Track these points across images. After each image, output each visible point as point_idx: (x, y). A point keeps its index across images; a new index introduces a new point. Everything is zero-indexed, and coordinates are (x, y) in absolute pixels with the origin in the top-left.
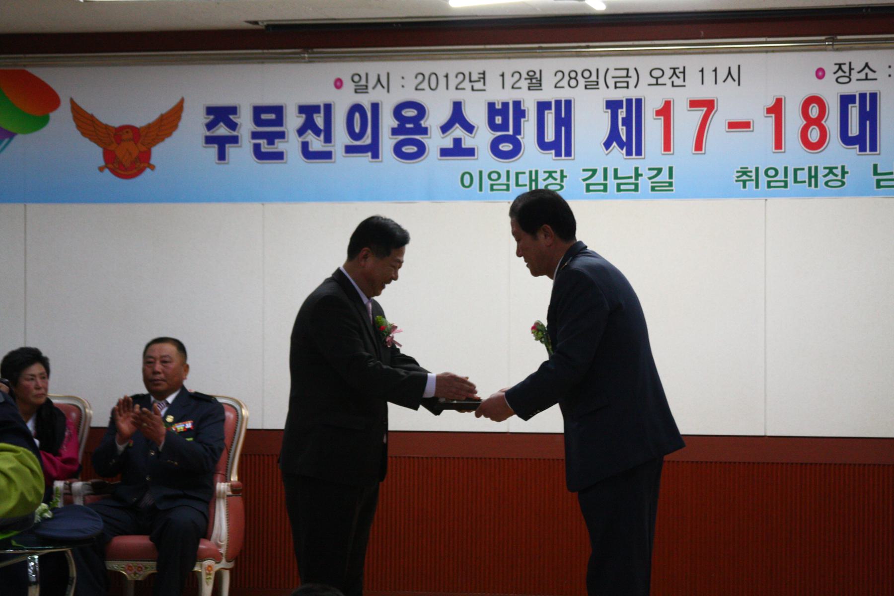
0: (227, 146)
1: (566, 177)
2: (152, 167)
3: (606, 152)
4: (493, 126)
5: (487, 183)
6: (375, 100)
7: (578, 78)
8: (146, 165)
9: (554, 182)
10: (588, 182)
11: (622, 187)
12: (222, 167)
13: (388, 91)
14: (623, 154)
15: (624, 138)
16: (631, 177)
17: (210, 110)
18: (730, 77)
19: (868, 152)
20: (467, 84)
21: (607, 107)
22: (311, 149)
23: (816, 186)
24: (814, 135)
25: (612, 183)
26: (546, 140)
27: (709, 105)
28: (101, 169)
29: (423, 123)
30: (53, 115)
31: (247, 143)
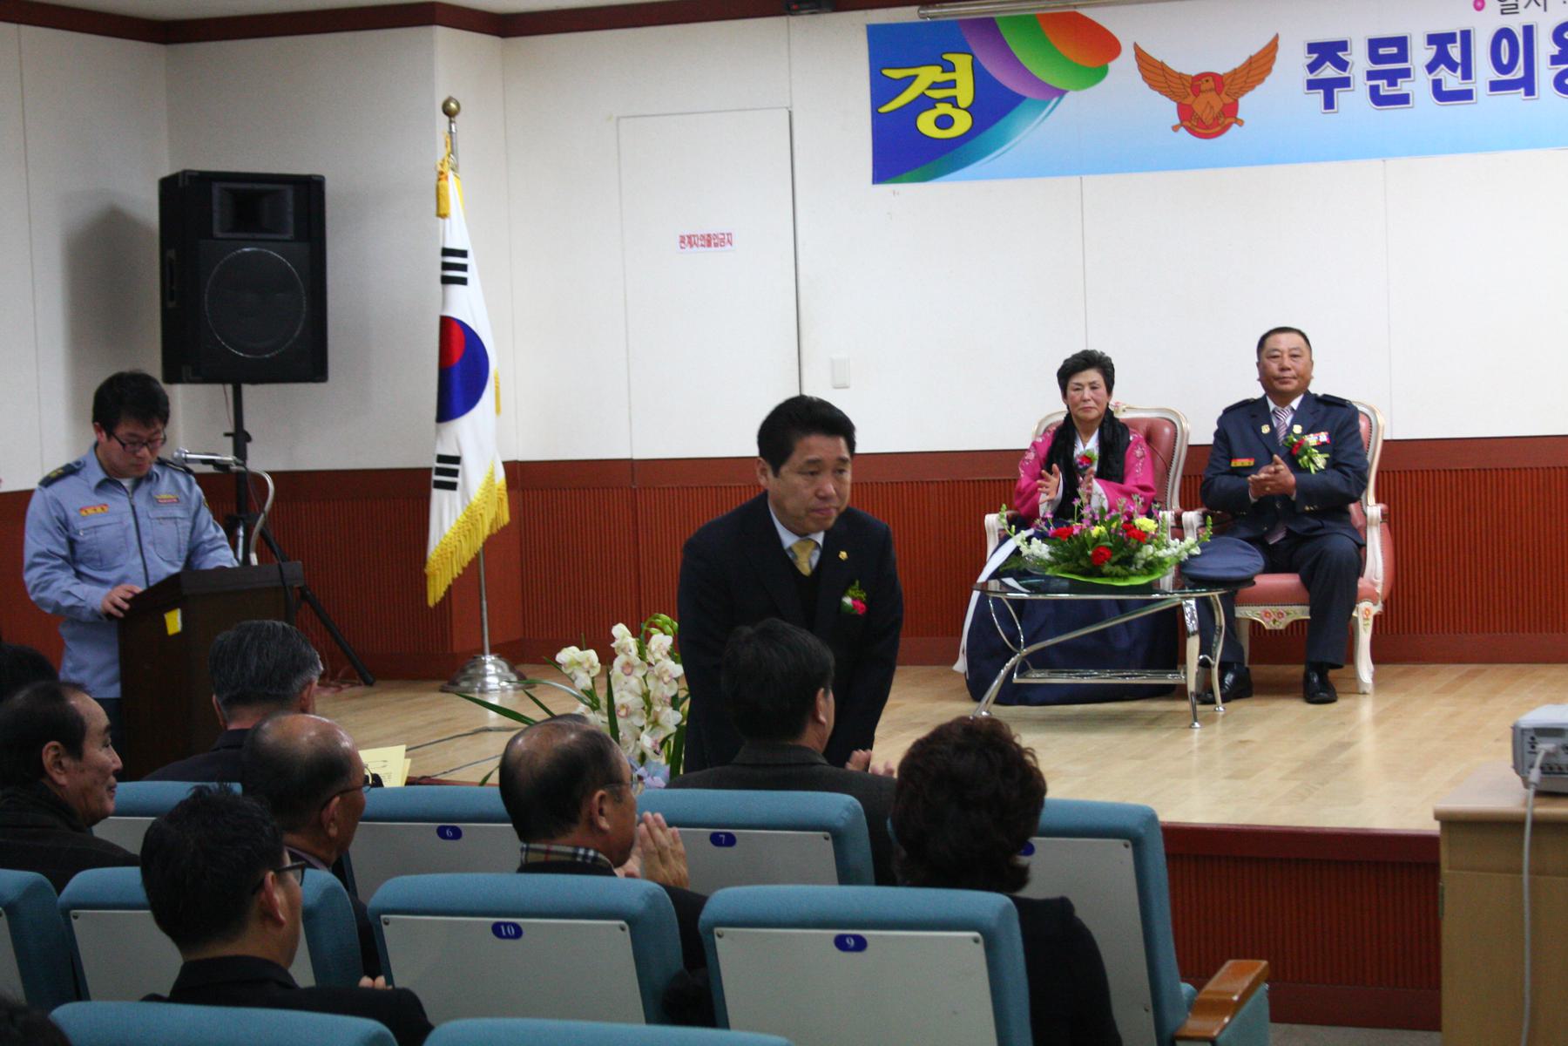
0: (1336, 90)
2: (1240, 123)
6: (1528, 22)
8: (1229, 120)
12: (1330, 116)
13: (1545, 10)
17: (1312, 48)
22: (1444, 89)
28: (1175, 129)
30: (1111, 65)
31: (1361, 85)
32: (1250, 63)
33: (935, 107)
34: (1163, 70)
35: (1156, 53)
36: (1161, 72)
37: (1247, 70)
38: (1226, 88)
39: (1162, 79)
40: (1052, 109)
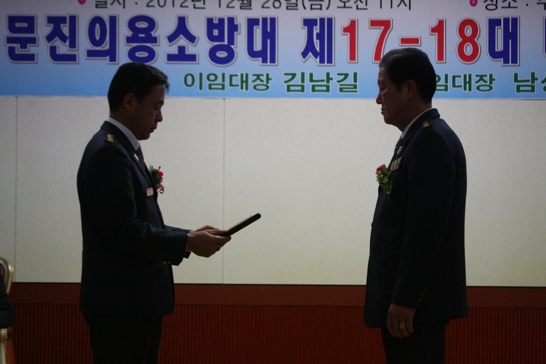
1: (271, 79)
3: (304, 60)
4: (211, 37)
5: (206, 83)
6: (113, 13)
9: (261, 83)
10: (289, 83)
11: (316, 88)
13: (124, 7)
14: (317, 62)
15: (318, 49)
16: (323, 81)
18: (402, 2)
19: (510, 64)
21: (305, 24)
22: (58, 53)
23: (470, 90)
24: (468, 50)
25: (308, 85)
26: (255, 50)
27: (386, 25)
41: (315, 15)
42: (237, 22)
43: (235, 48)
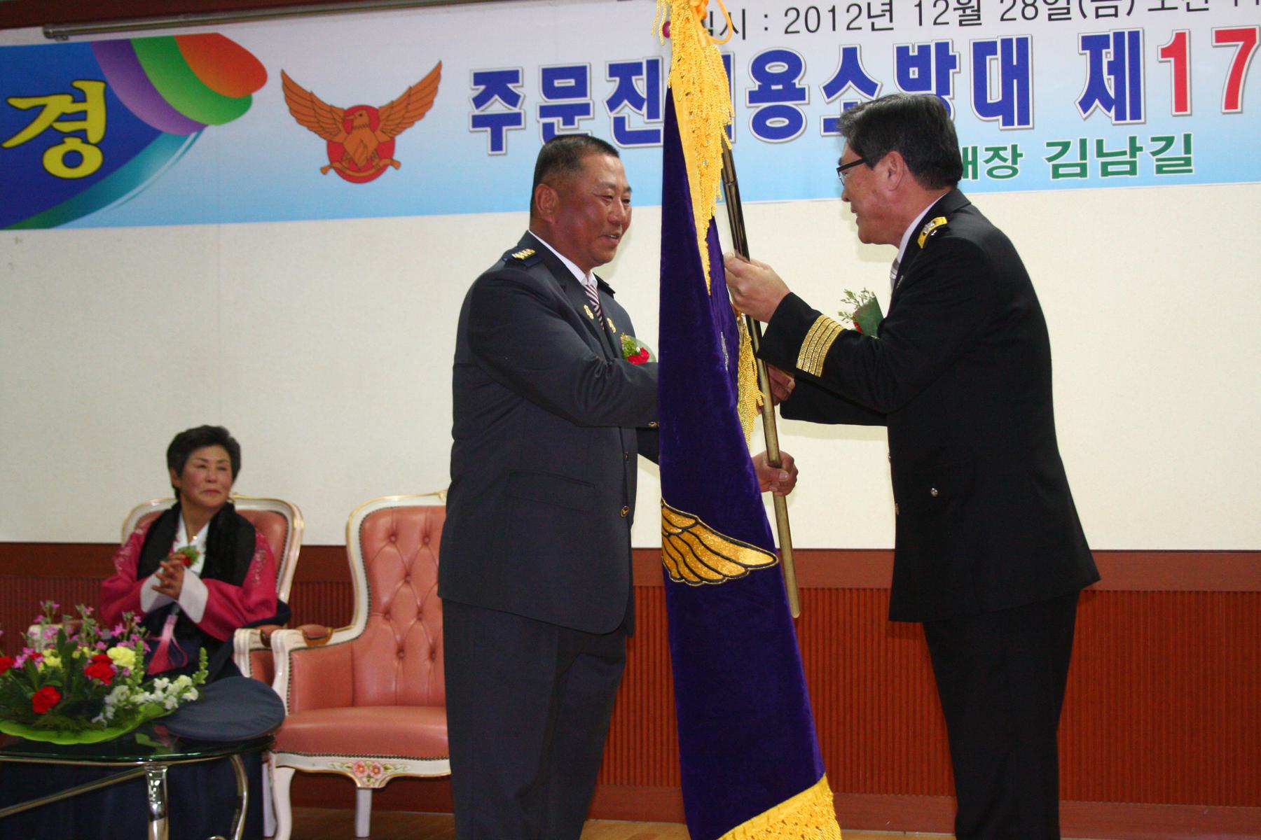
0: (505, 128)
1: (1021, 155)
2: (397, 165)
3: (1084, 116)
7: (1036, 4)
8: (387, 161)
9: (1002, 164)
10: (1055, 162)
11: (1110, 169)
12: (498, 159)
13: (744, 37)
15: (1112, 93)
16: (1124, 153)
17: (479, 78)
20: (864, 21)
21: (1084, 48)
22: (627, 129)
25: (1094, 162)
26: (989, 101)
28: (324, 171)
29: (798, 83)
30: (257, 96)
32: (409, 96)
33: (63, 142)
34: (312, 102)
35: (306, 82)
36: (308, 104)
37: (404, 104)
38: (381, 124)
39: (312, 113)
40: (188, 148)
41: (1106, 27)
42: (953, 51)
43: (950, 99)
